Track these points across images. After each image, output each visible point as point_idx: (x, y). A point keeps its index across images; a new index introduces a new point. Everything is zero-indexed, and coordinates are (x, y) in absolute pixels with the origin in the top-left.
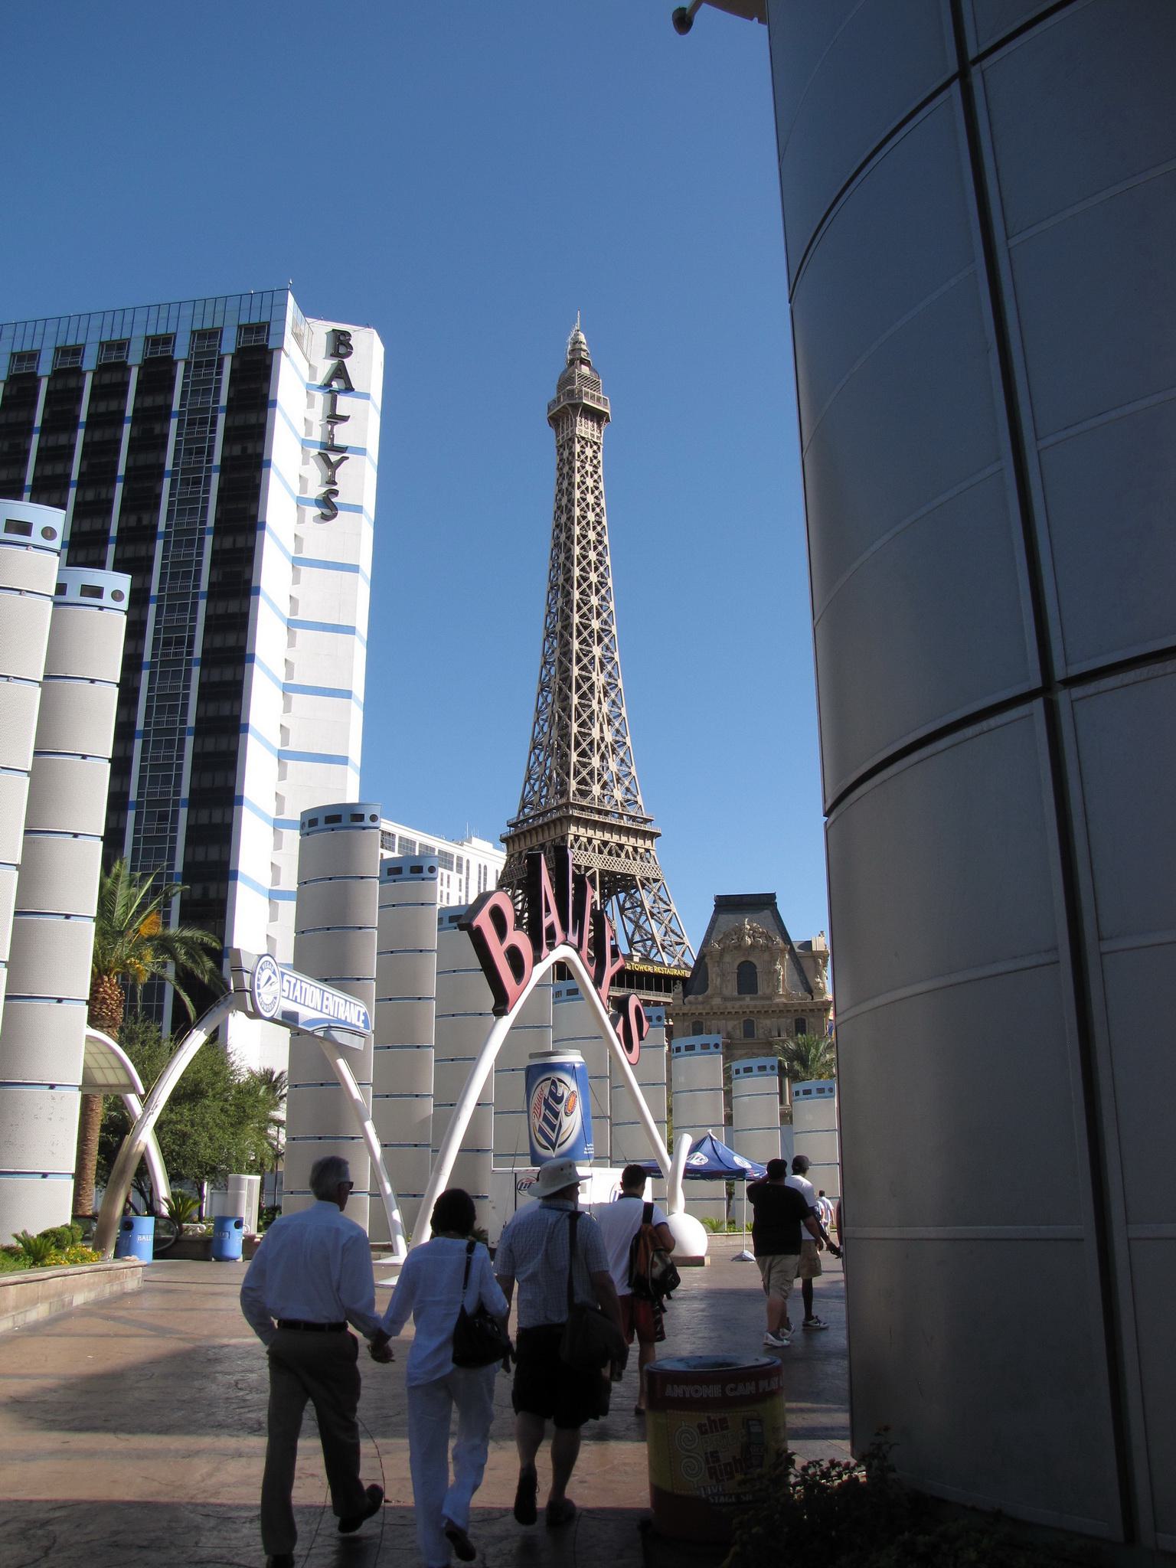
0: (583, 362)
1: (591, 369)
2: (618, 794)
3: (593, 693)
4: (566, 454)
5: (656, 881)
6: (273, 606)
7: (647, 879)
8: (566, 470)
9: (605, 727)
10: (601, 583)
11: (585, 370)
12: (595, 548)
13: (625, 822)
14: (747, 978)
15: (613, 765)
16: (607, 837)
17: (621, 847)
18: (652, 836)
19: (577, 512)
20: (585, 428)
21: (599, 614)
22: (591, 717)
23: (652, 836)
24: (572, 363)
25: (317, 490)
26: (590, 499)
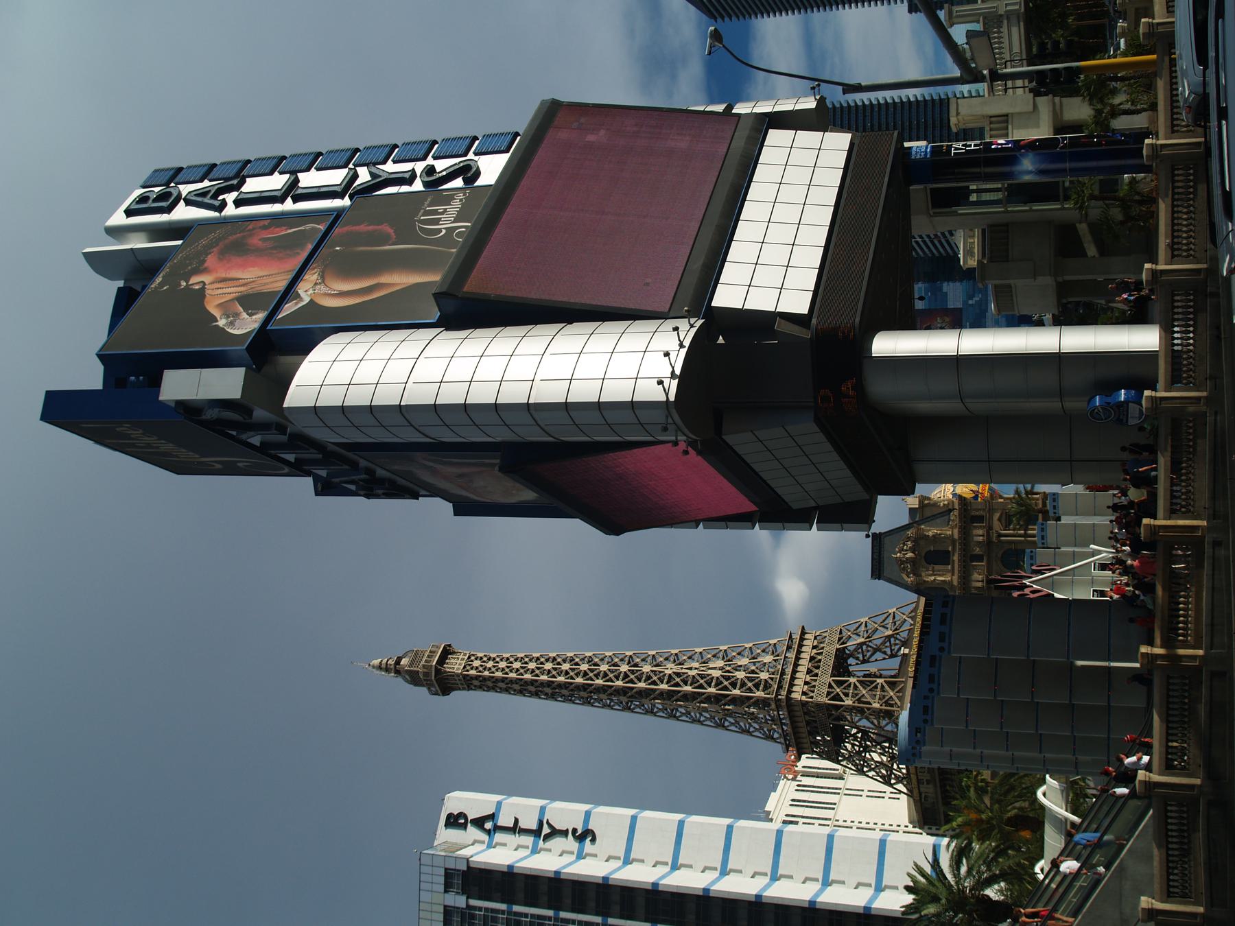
2: (768, 659)
4: (476, 683)
6: (663, 877)
7: (840, 639)
8: (490, 684)
11: (404, 662)
12: (559, 664)
13: (792, 655)
15: (744, 661)
17: (812, 658)
18: (803, 633)
19: (528, 676)
20: (455, 665)
21: (615, 665)
22: (702, 677)
23: (803, 633)
24: (398, 672)
25: (571, 843)
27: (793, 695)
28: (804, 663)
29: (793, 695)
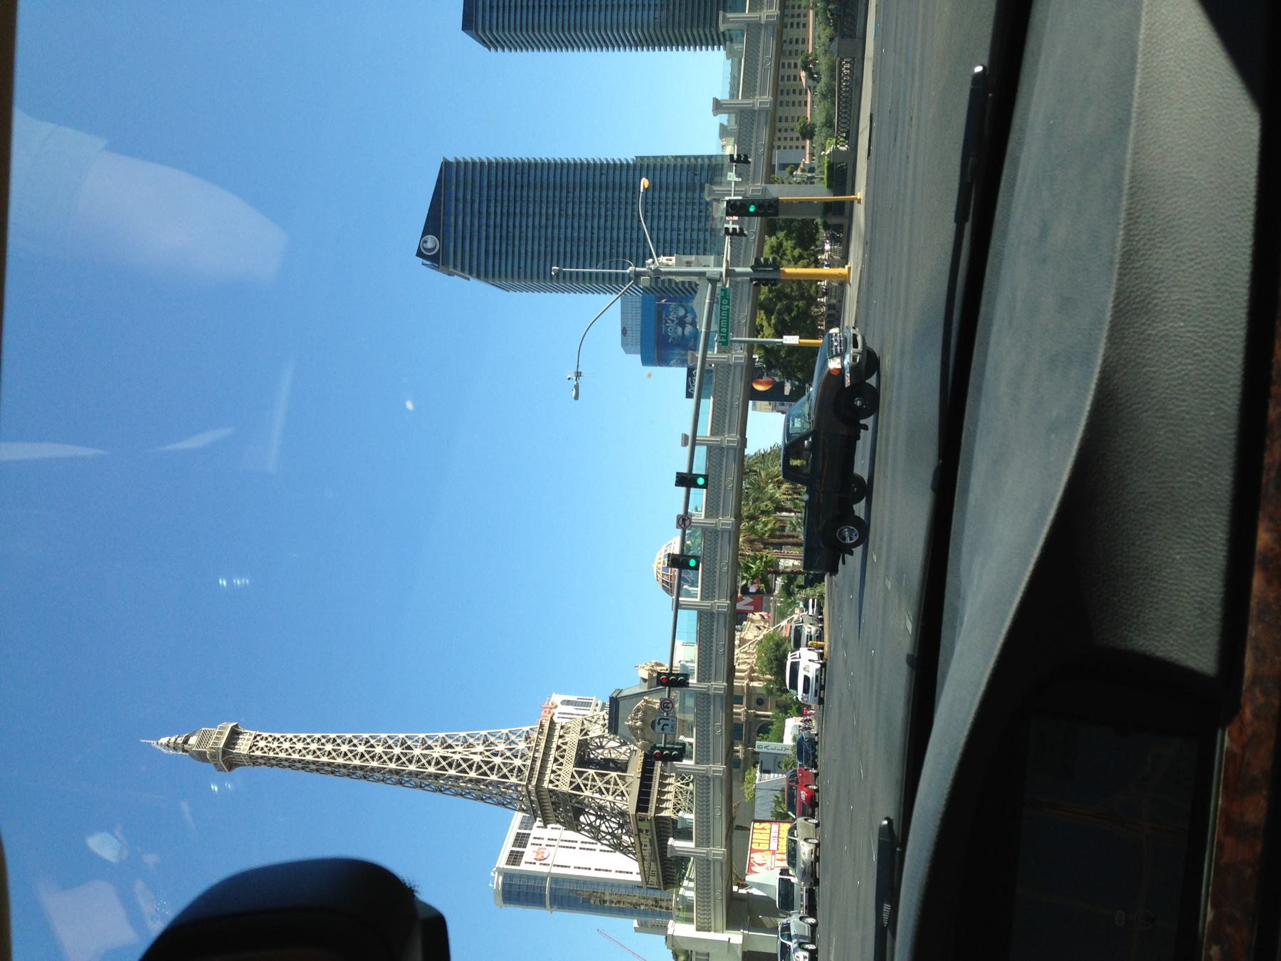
0: (186, 742)
1: (193, 734)
9: (473, 750)
11: (193, 740)
15: (501, 747)
16: (551, 759)
17: (559, 747)
20: (243, 747)
22: (465, 760)
23: (552, 723)
26: (300, 746)
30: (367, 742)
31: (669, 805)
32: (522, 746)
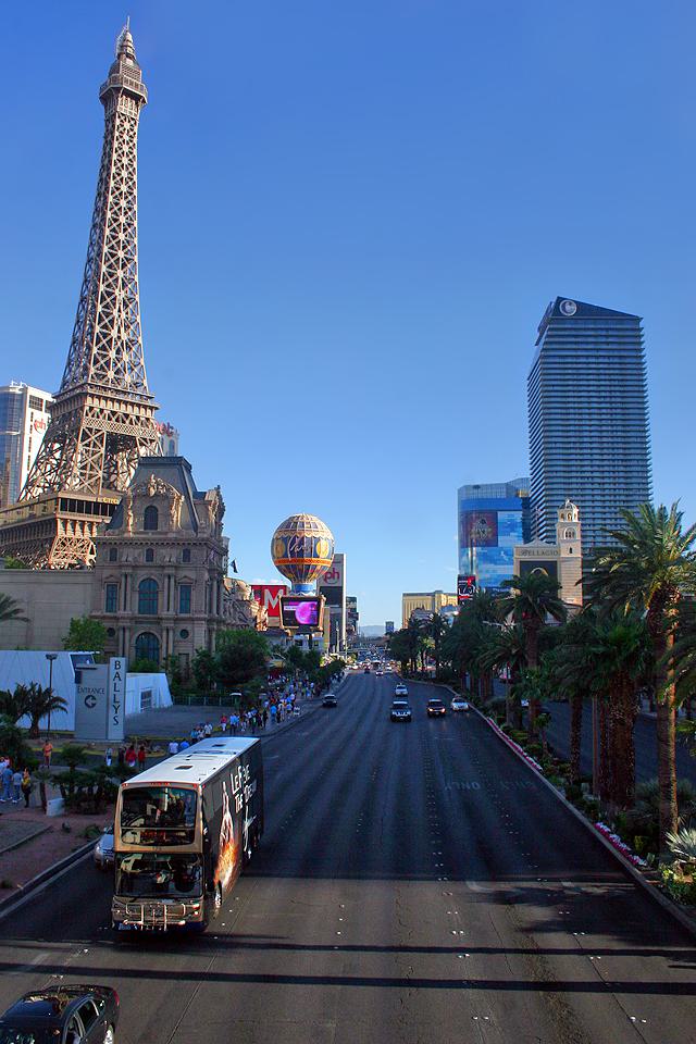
0: (128, 56)
3: (114, 304)
4: (110, 126)
5: (152, 441)
7: (145, 440)
8: (109, 138)
9: (122, 329)
10: (129, 225)
11: (130, 62)
14: (151, 518)
15: (126, 357)
16: (116, 407)
17: (127, 416)
20: (125, 106)
22: (112, 322)
27: (89, 399)
28: (122, 409)
29: (89, 399)
30: (129, 225)
31: (70, 534)
32: (128, 378)
